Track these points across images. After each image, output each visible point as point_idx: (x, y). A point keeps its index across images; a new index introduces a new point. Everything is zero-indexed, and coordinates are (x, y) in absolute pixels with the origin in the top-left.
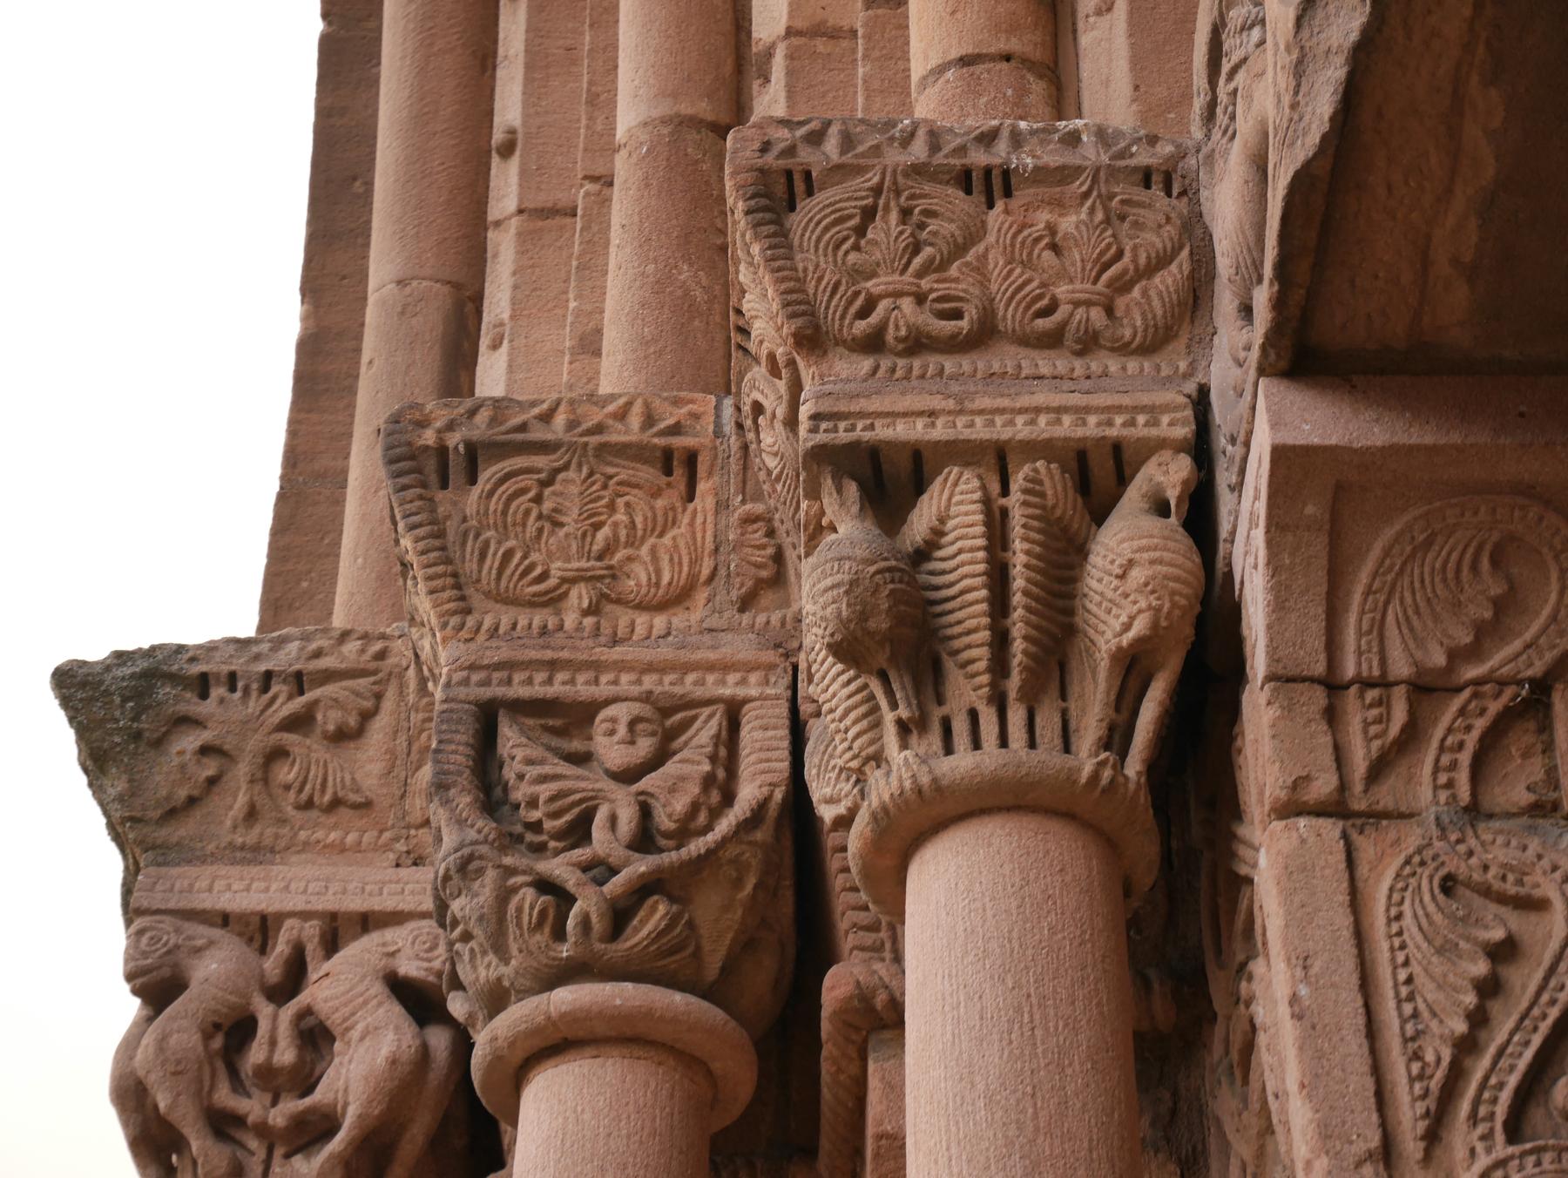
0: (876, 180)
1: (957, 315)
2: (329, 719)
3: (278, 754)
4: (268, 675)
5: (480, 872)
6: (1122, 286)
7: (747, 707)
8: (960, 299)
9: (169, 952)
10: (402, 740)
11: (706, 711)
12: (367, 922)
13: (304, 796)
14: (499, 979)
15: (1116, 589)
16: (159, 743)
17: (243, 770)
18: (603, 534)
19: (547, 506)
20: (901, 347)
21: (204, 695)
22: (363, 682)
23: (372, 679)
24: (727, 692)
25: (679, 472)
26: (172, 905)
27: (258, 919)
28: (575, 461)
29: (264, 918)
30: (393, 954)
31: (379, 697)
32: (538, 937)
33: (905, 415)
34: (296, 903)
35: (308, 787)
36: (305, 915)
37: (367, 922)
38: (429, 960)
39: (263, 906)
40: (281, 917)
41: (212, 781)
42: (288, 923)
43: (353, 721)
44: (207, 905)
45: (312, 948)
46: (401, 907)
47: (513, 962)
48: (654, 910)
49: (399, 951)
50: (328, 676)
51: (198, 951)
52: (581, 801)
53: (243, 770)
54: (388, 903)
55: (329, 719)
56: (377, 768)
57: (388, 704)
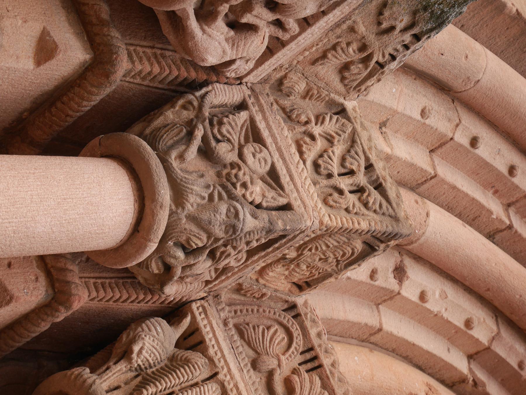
3: (363, 48)
5: (226, 232)
13: (339, 49)
14: (183, 208)
16: (415, 13)
27: (311, 23)
31: (345, 86)
32: (184, 238)
35: (340, 51)
36: (294, 38)
41: (379, 23)
43: (346, 74)
47: (184, 220)
48: (158, 269)
53: (371, 38)
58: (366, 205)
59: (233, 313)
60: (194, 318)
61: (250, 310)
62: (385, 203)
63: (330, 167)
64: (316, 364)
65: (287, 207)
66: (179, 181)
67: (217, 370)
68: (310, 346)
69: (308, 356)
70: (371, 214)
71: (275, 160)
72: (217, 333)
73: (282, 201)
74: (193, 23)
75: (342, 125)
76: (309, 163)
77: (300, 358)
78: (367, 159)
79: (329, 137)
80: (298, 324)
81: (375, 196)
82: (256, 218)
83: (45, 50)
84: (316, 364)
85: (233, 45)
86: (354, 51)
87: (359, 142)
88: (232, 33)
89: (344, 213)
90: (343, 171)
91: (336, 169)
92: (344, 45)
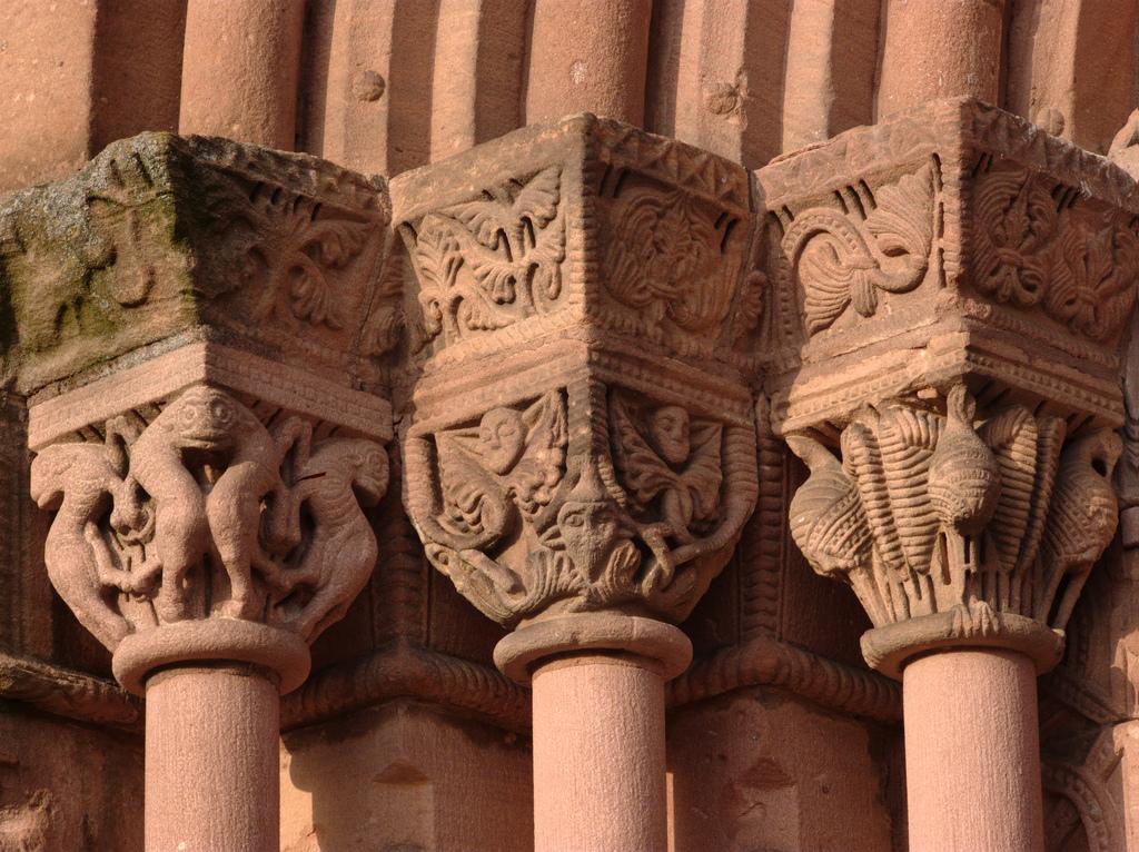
0: (1023, 178)
1: (1031, 288)
2: (332, 250)
3: (297, 270)
4: (300, 199)
6: (1106, 296)
7: (733, 430)
8: (1039, 280)
9: (233, 427)
10: (372, 282)
11: (715, 426)
12: (338, 432)
15: (1085, 525)
17: (275, 275)
18: (682, 266)
19: (659, 234)
20: (1003, 300)
21: (253, 198)
22: (357, 227)
23: (363, 226)
24: (727, 415)
25: (723, 229)
26: (229, 384)
28: (678, 205)
29: (280, 410)
30: (357, 467)
31: (364, 242)
33: (1006, 360)
34: (301, 405)
35: (310, 305)
36: (305, 416)
37: (338, 432)
38: (378, 479)
39: (283, 402)
40: (295, 412)
42: (294, 420)
44: (250, 390)
45: (305, 443)
46: (361, 427)
49: (361, 466)
50: (339, 214)
51: (250, 430)
52: (660, 484)
54: (351, 421)
55: (332, 250)
56: (351, 301)
57: (369, 251)
58: (547, 220)
59: (790, 337)
60: (794, 432)
61: (783, 304)
62: (538, 181)
63: (499, 281)
64: (859, 189)
65: (563, 393)
66: (543, 597)
67: (865, 406)
68: (833, 196)
69: (849, 202)
70: (560, 208)
71: (500, 399)
72: (815, 390)
73: (555, 398)
74: (319, 605)
75: (431, 234)
76: (500, 315)
77: (854, 216)
78: (476, 198)
79: (454, 266)
80: (800, 211)
81: (532, 200)
82: (579, 476)
83: (406, 776)
84: (859, 189)
85: (337, 524)
86: (304, 281)
87: (452, 209)
88: (320, 531)
89: (563, 267)
90: (502, 248)
91: (499, 266)
92: (298, 306)
